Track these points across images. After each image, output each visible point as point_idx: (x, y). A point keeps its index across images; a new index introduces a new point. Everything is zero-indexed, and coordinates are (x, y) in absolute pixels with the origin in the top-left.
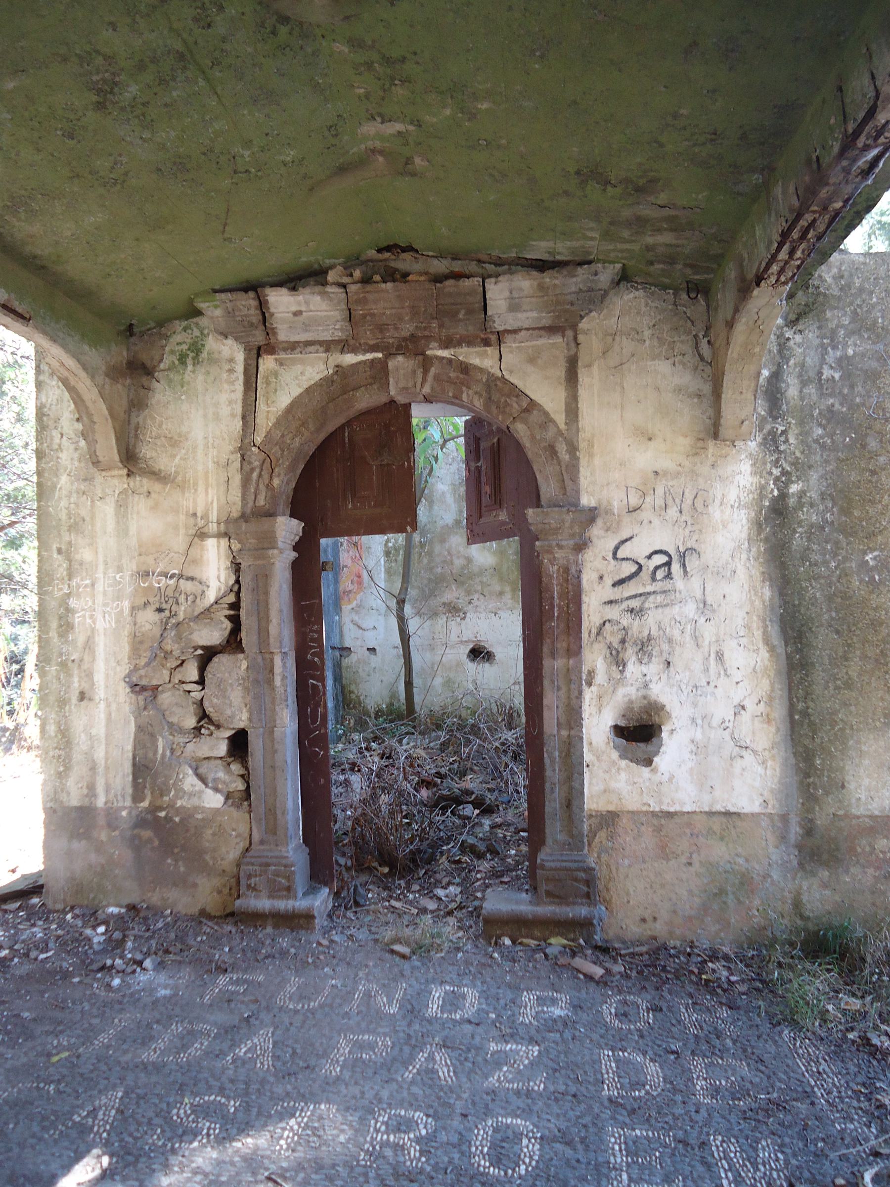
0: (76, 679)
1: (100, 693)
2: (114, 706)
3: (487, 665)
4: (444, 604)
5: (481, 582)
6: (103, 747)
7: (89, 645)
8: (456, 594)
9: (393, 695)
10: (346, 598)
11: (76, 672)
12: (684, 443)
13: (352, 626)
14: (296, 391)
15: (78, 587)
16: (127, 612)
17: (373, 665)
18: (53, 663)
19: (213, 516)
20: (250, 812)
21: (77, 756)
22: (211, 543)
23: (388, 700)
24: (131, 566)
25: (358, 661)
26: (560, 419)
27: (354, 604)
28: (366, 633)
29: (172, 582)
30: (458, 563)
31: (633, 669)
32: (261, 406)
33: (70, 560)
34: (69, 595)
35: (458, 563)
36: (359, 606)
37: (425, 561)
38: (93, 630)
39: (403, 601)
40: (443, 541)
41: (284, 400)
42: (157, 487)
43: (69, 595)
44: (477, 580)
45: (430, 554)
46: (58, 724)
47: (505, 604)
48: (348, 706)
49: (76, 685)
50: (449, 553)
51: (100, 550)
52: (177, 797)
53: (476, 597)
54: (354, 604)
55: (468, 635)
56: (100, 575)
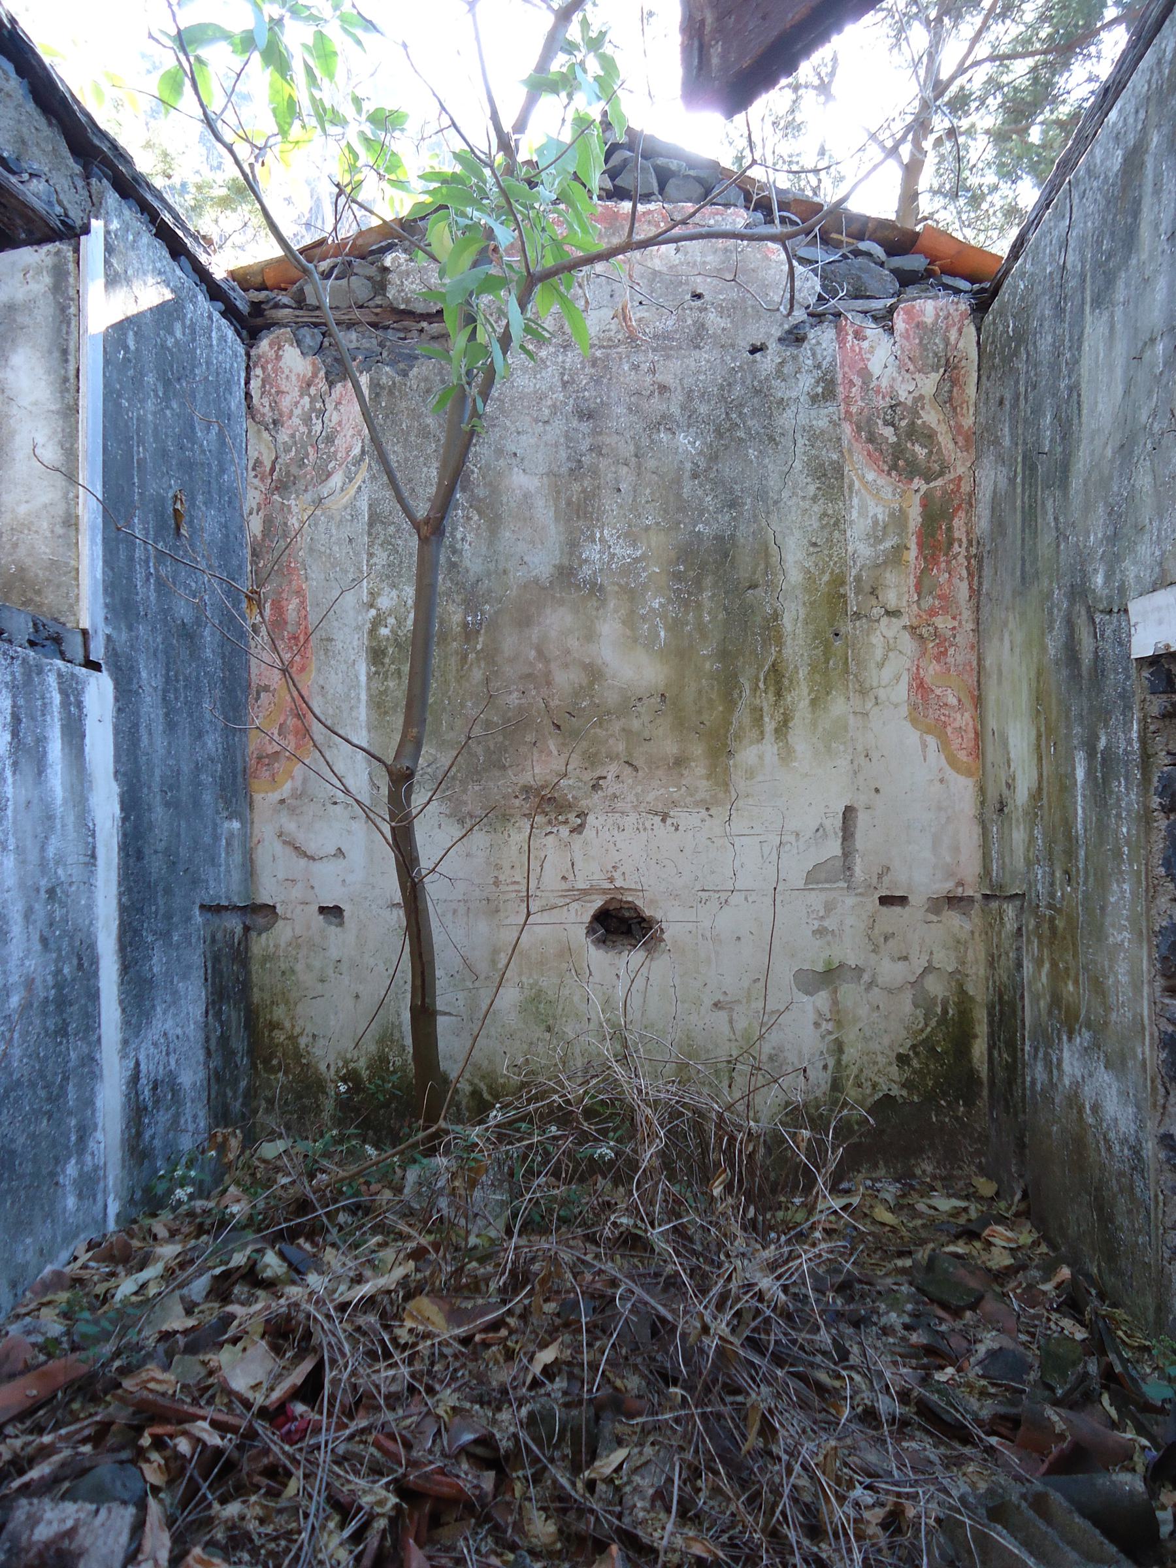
3: (637, 956)
4: (526, 789)
5: (627, 731)
8: (557, 764)
9: (386, 1038)
10: (265, 774)
13: (278, 847)
17: (334, 953)
23: (373, 1048)
25: (296, 942)
27: (286, 789)
28: (316, 867)
30: (565, 679)
35: (565, 679)
36: (298, 795)
37: (477, 675)
39: (409, 775)
40: (524, 621)
44: (616, 726)
45: (490, 656)
47: (691, 792)
48: (266, 1061)
50: (540, 653)
53: (611, 770)
54: (286, 789)
55: (590, 873)
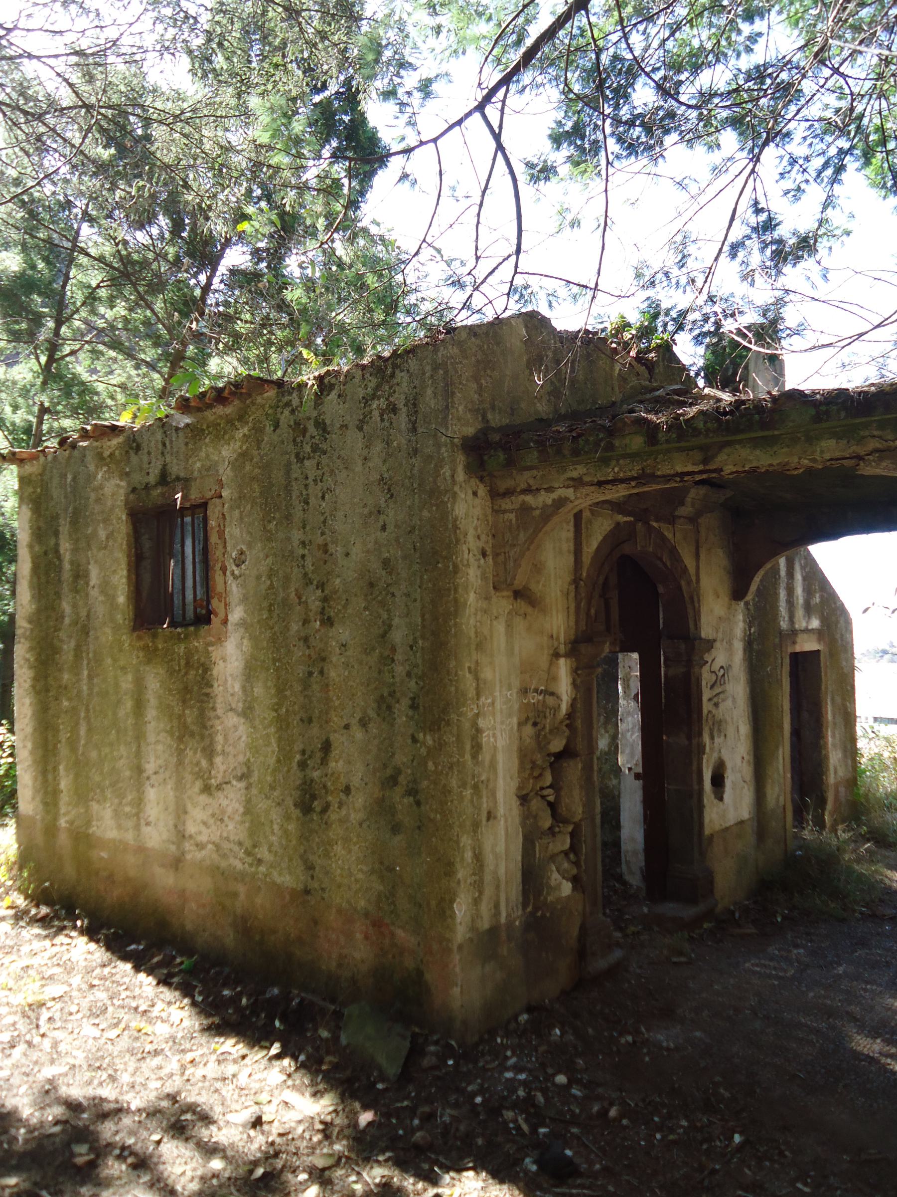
0: (485, 800)
1: (501, 811)
2: (510, 820)
6: (504, 863)
7: (493, 765)
11: (484, 792)
12: (727, 599)
14: (600, 538)
15: (484, 705)
16: (515, 727)
18: (469, 786)
19: (562, 639)
20: (584, 893)
21: (488, 878)
22: (562, 661)
24: (516, 684)
26: (694, 578)
29: (541, 698)
31: (716, 740)
32: (585, 549)
33: (477, 679)
34: (477, 715)
38: (495, 748)
41: (594, 544)
42: (529, 610)
43: (477, 715)
46: (474, 849)
49: (485, 805)
51: (497, 669)
52: (548, 894)
56: (497, 694)
